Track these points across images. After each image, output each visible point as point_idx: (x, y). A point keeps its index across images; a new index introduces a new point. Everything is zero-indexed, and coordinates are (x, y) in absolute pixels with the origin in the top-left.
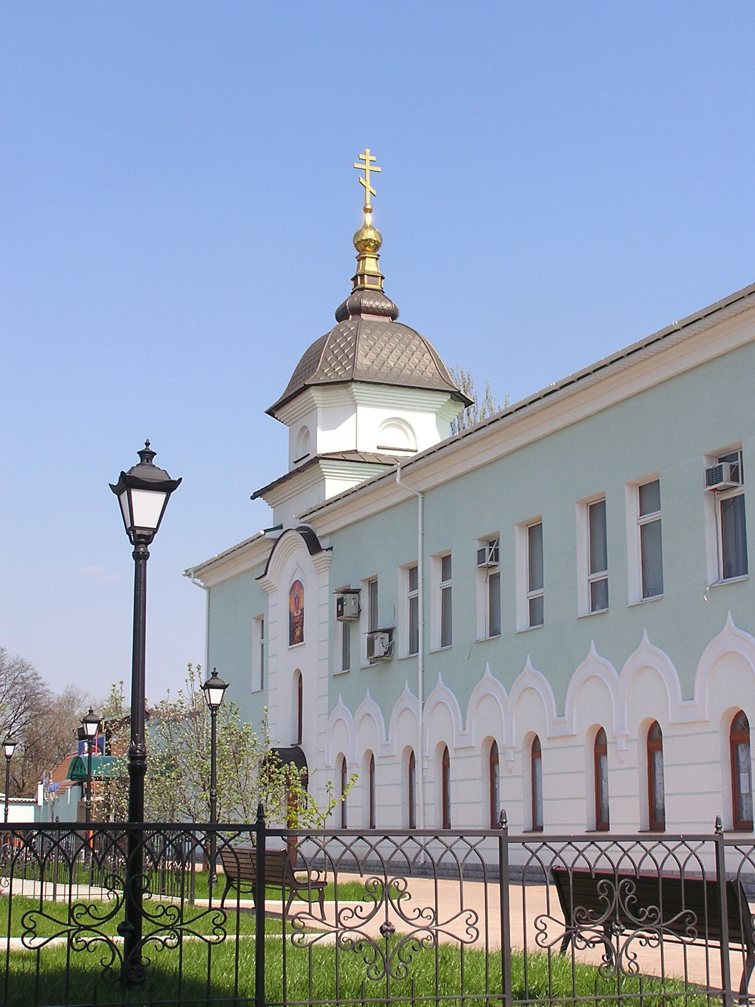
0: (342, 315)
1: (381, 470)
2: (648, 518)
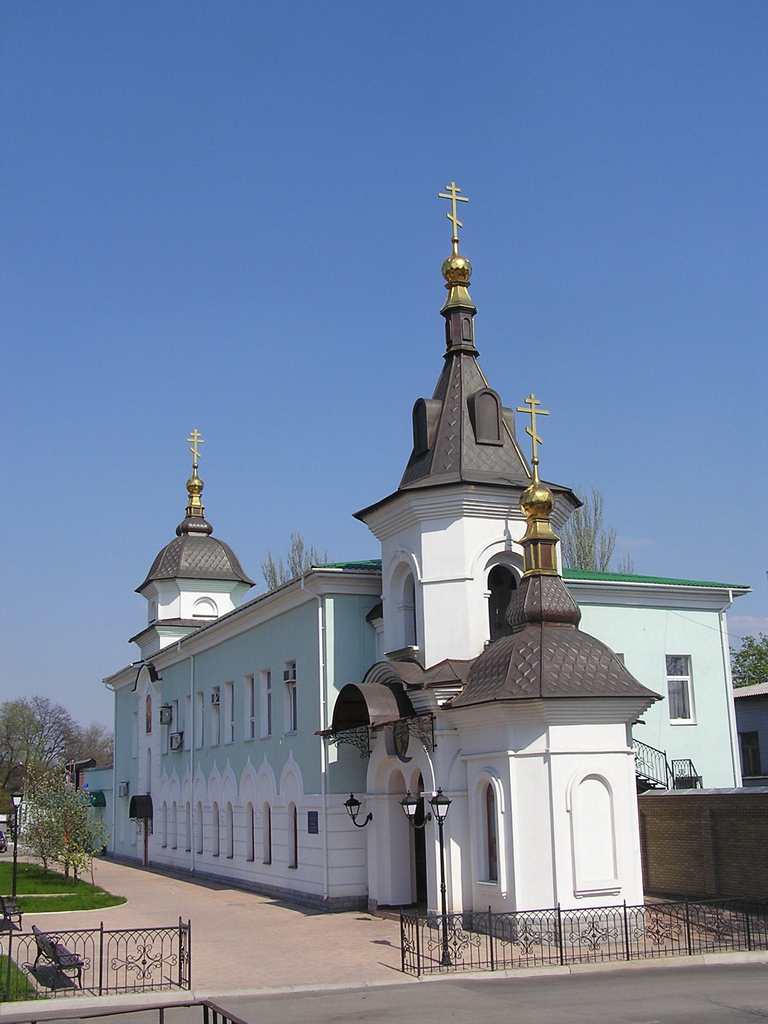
0: (178, 532)
1: (193, 630)
2: (270, 691)
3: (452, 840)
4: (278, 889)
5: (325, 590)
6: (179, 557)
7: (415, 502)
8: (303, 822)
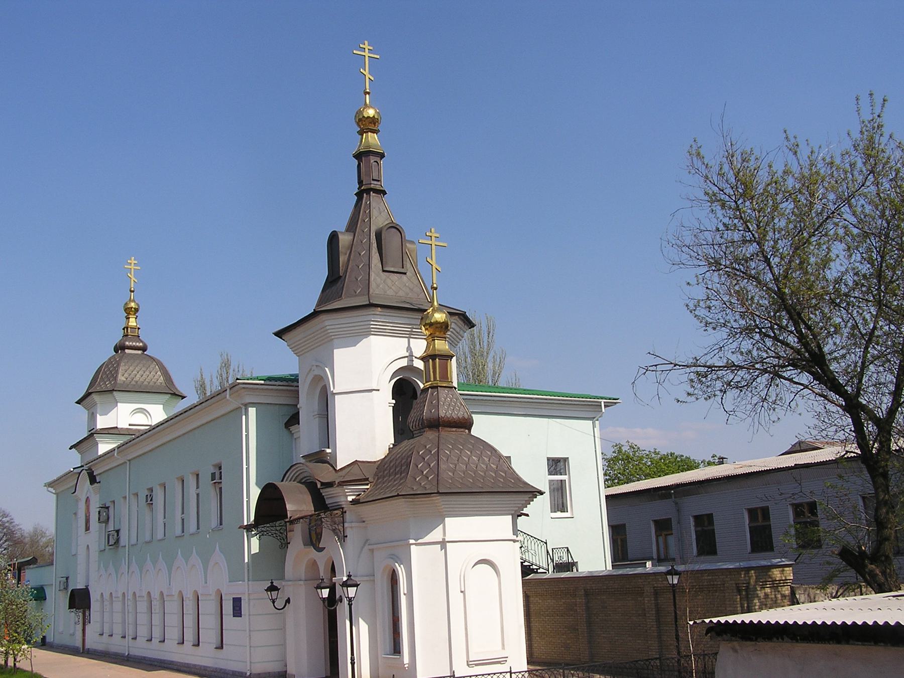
0: (116, 350)
1: (128, 438)
3: (360, 619)
4: (205, 668)
5: (248, 400)
6: (117, 372)
7: (328, 322)
8: (228, 607)
